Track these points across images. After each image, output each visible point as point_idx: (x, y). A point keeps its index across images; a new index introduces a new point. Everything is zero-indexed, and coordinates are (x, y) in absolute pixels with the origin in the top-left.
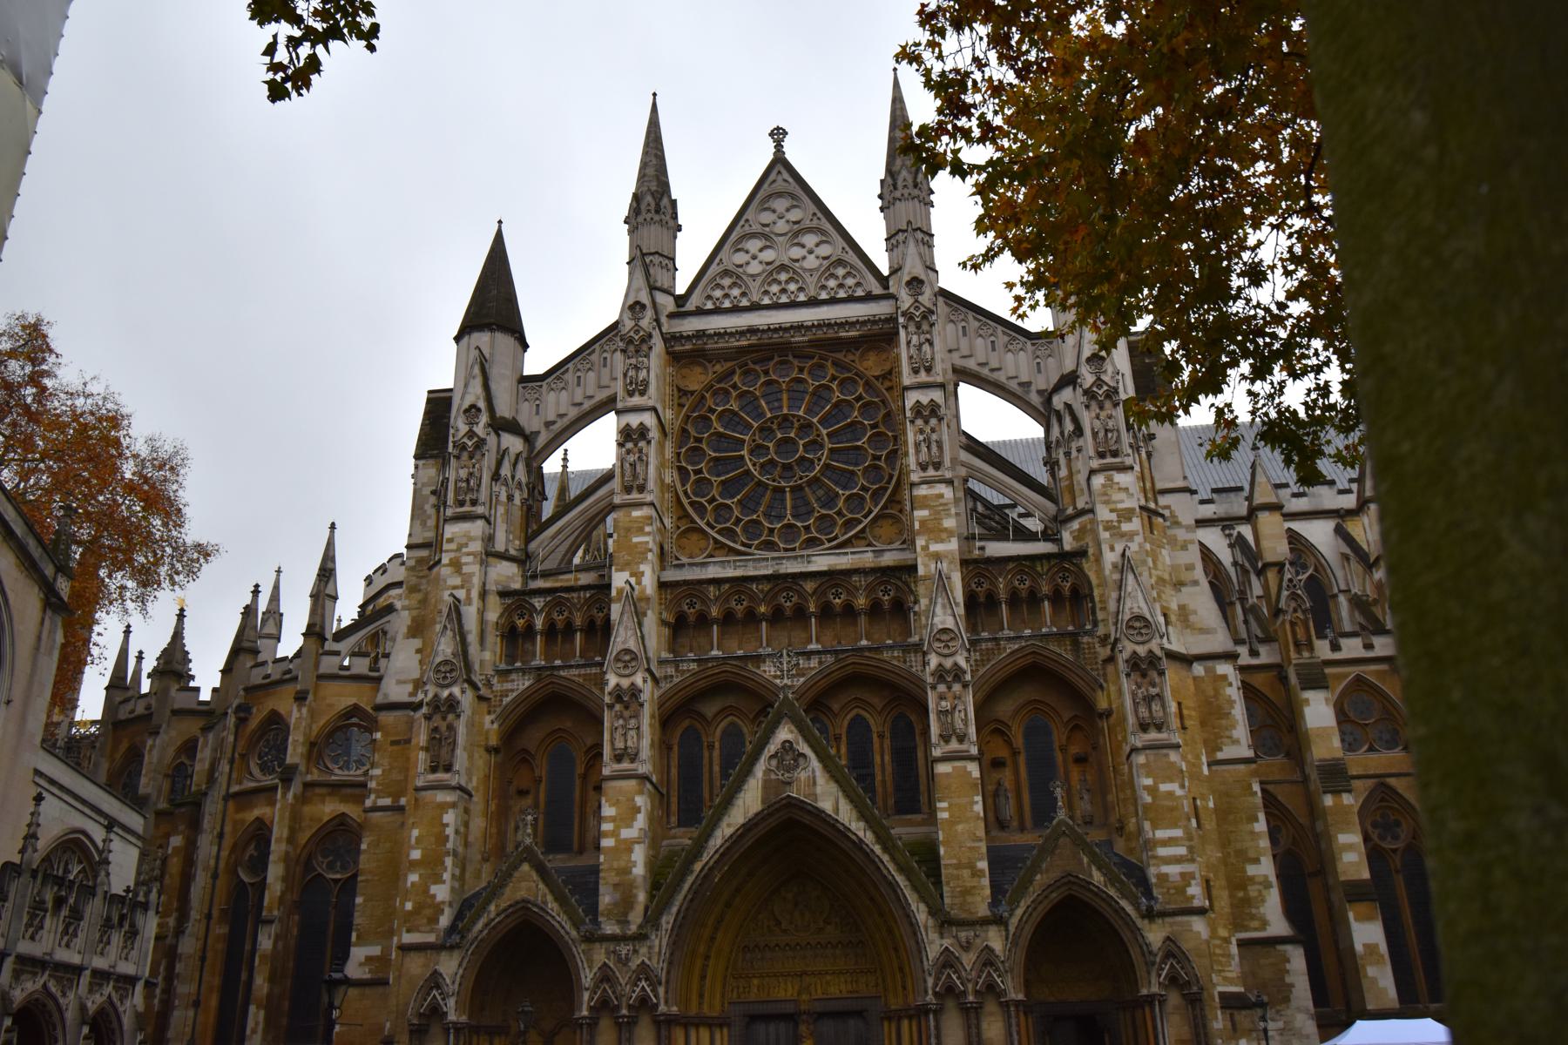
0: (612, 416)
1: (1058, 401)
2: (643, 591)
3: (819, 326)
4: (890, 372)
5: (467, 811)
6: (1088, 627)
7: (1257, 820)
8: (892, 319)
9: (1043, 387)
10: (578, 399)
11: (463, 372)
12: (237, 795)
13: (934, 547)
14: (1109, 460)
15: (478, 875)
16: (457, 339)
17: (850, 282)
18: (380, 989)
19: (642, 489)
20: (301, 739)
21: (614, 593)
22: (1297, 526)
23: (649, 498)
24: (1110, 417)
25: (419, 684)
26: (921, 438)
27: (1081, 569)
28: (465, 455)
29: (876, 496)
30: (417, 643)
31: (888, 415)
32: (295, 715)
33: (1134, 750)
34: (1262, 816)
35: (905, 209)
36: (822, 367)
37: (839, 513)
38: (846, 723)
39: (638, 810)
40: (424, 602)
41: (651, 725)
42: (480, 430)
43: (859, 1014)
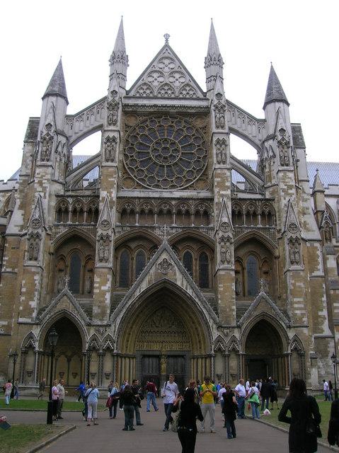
0: (99, 133)
2: (112, 199)
3: (181, 107)
8: (207, 107)
16: (43, 99)
17: (191, 92)
18: (6, 338)
19: (112, 161)
21: (100, 199)
25: (22, 227)
27: (271, 205)
28: (45, 142)
30: (22, 212)
31: (204, 142)
33: (288, 270)
35: (214, 69)
37: (184, 177)
40: (26, 196)
43: (183, 356)
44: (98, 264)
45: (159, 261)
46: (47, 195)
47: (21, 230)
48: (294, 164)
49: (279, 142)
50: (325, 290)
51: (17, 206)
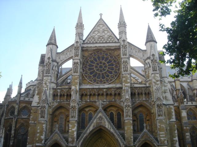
0: (72, 60)
1: (147, 62)
2: (77, 89)
4: (119, 55)
5: (47, 124)
6: (150, 99)
7: (175, 131)
8: (119, 46)
9: (144, 59)
10: (66, 57)
11: (47, 51)
12: (6, 119)
13: (126, 85)
14: (155, 72)
15: (48, 134)
16: (47, 46)
17: (112, 39)
19: (77, 72)
20: (17, 110)
21: (72, 90)
22: (181, 83)
23: (78, 74)
24: (155, 65)
25: (38, 103)
26: (124, 66)
27: (149, 89)
28: (48, 65)
29: (116, 76)
30: (38, 96)
31: (118, 62)
32: (17, 107)
33: (157, 119)
34: (176, 130)
35: (122, 28)
36: (107, 54)
37: (110, 78)
38: (109, 113)
39: (75, 126)
40: (40, 89)
41: (78, 112)
42: (50, 61)
44: (71, 119)
45: (98, 117)
46: (49, 89)
47: (38, 105)
48: (159, 70)
49: (152, 61)
50: (176, 128)
51: (36, 94)
